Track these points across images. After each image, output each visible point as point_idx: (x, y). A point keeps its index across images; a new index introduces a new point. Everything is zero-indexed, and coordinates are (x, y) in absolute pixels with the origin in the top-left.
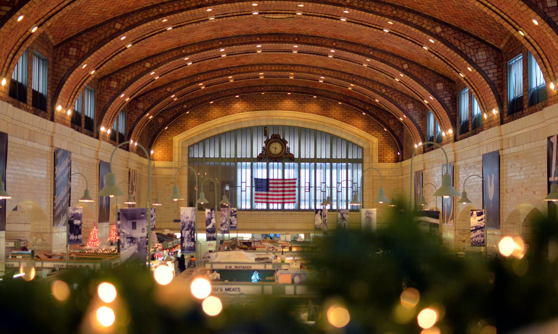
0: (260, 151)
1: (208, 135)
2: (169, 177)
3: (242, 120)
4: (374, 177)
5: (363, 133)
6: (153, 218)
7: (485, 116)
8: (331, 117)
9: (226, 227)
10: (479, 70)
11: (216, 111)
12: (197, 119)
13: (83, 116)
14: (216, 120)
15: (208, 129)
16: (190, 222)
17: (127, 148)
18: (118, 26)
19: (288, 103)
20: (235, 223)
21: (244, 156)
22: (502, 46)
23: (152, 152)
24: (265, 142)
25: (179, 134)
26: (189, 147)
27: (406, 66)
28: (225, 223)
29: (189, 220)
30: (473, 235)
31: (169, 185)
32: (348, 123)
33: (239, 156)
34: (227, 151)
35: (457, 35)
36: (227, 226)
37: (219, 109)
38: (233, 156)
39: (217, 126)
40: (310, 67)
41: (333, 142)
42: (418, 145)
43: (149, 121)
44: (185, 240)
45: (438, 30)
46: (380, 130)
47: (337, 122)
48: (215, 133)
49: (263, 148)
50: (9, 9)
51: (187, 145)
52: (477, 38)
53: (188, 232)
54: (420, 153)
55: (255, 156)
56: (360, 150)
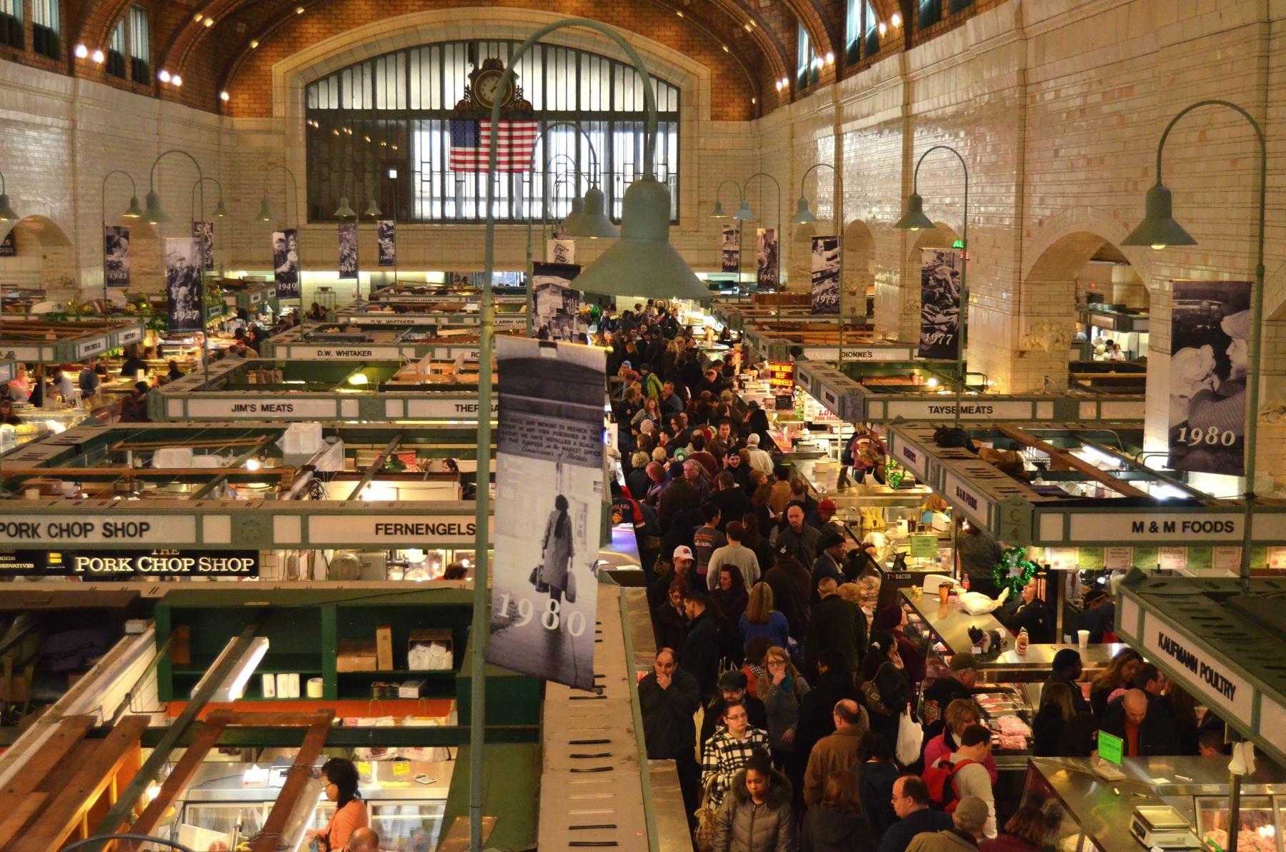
0: (460, 96)
1: (347, 61)
2: (266, 153)
4: (702, 153)
5: (678, 57)
7: (883, 29)
9: (351, 265)
12: (322, 26)
13: (26, 25)
14: (362, 27)
16: (188, 267)
17: (158, 91)
20: (391, 251)
21: (425, 107)
23: (225, 96)
24: (470, 76)
25: (284, 57)
28: (349, 255)
29: (185, 264)
30: (817, 289)
32: (647, 36)
33: (415, 106)
34: (389, 95)
36: (353, 262)
38: (403, 107)
41: (616, 76)
42: (782, 84)
43: (207, 31)
44: (179, 306)
46: (715, 49)
48: (363, 55)
49: (466, 88)
51: (301, 84)
53: (183, 290)
54: (786, 103)
55: (449, 106)
56: (673, 93)
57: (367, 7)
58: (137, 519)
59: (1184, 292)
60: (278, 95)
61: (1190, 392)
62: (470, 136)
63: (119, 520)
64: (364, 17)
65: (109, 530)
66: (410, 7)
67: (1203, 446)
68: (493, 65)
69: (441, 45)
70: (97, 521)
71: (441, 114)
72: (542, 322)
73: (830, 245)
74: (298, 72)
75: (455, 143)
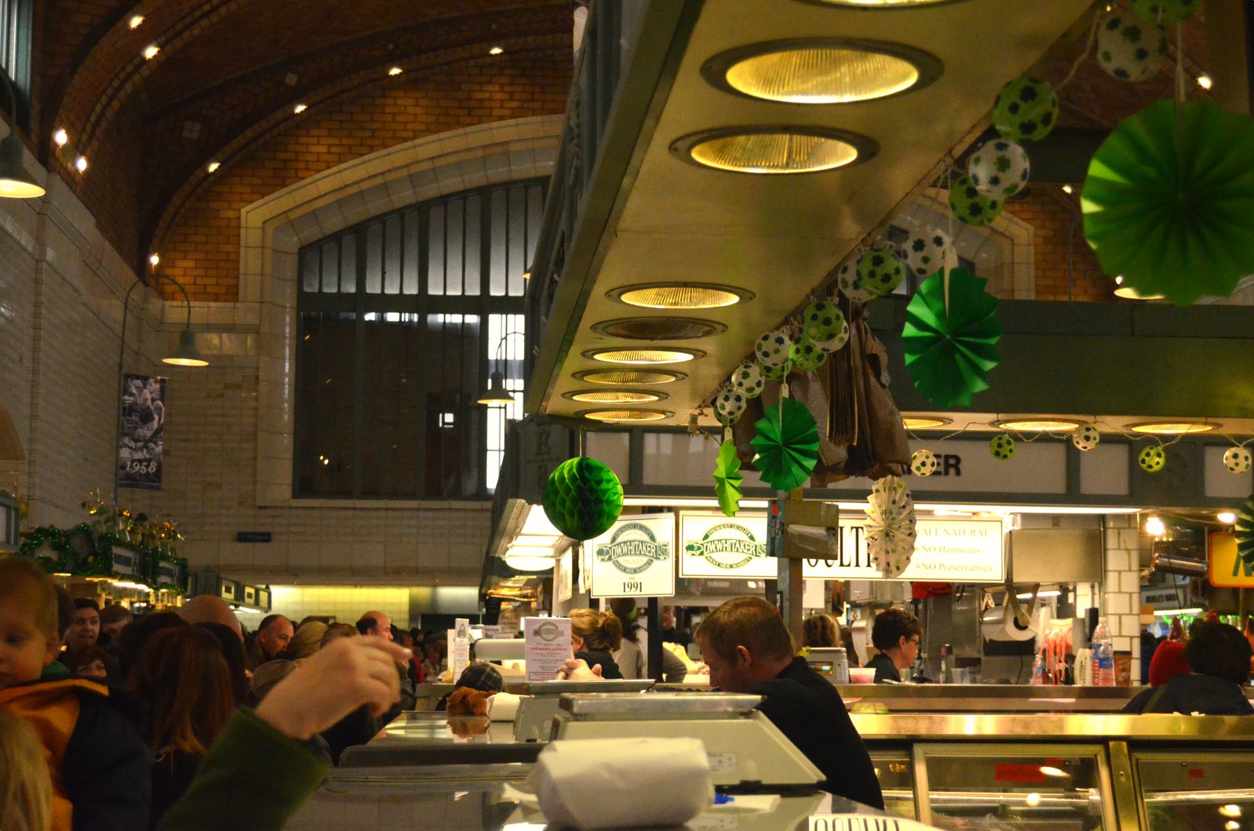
1: (377, 206)
3: (513, 147)
6: (155, 425)
11: (408, 106)
12: (336, 141)
14: (409, 144)
15: (379, 180)
25: (263, 196)
26: (303, 251)
31: (222, 396)
37: (425, 102)
39: (414, 169)
43: (145, 72)
51: (293, 243)
57: (418, 110)
60: (250, 261)
64: (413, 126)
66: (496, 112)
74: (285, 222)
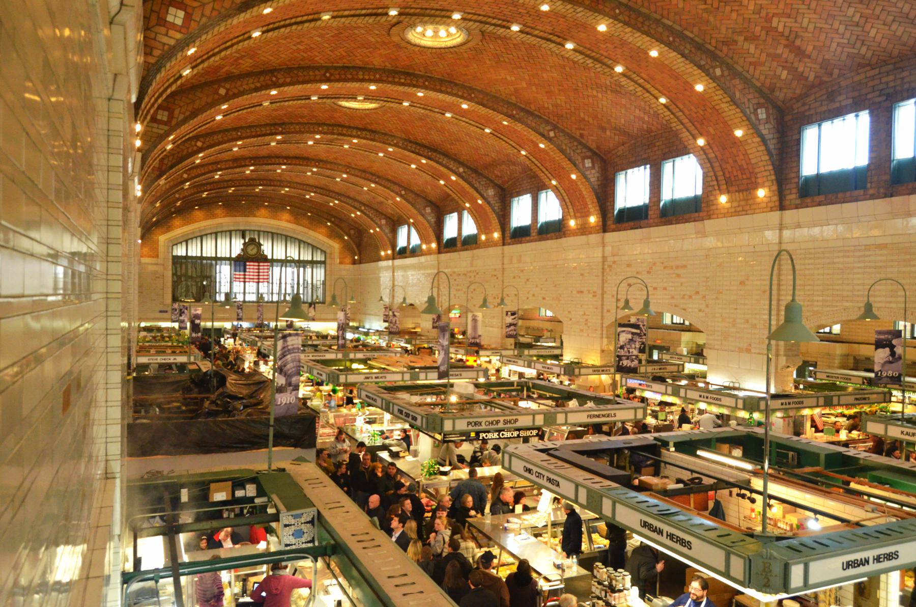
1: (191, 236)
2: (155, 272)
5: (326, 240)
7: (483, 237)
8: (300, 225)
10: (489, 203)
18: (199, 144)
19: (263, 211)
22: (506, 186)
27: (403, 192)
33: (219, 255)
34: (208, 249)
35: (474, 175)
40: (304, 185)
45: (461, 170)
46: (341, 238)
47: (306, 230)
48: (198, 234)
50: (166, 128)
52: (487, 178)
55: (234, 256)
58: (514, 418)
59: (879, 333)
60: (161, 249)
61: (882, 361)
62: (242, 268)
63: (508, 418)
65: (506, 422)
67: (887, 377)
68: (252, 240)
69: (230, 232)
70: (502, 419)
71: (230, 259)
72: (622, 344)
73: (513, 314)
74: (170, 240)
75: (235, 271)
